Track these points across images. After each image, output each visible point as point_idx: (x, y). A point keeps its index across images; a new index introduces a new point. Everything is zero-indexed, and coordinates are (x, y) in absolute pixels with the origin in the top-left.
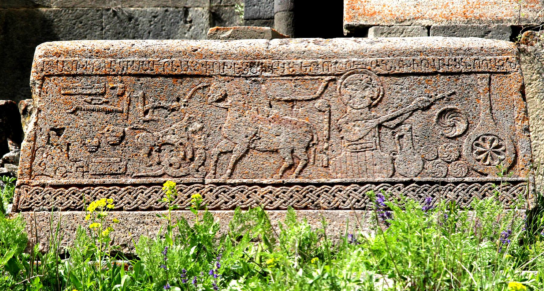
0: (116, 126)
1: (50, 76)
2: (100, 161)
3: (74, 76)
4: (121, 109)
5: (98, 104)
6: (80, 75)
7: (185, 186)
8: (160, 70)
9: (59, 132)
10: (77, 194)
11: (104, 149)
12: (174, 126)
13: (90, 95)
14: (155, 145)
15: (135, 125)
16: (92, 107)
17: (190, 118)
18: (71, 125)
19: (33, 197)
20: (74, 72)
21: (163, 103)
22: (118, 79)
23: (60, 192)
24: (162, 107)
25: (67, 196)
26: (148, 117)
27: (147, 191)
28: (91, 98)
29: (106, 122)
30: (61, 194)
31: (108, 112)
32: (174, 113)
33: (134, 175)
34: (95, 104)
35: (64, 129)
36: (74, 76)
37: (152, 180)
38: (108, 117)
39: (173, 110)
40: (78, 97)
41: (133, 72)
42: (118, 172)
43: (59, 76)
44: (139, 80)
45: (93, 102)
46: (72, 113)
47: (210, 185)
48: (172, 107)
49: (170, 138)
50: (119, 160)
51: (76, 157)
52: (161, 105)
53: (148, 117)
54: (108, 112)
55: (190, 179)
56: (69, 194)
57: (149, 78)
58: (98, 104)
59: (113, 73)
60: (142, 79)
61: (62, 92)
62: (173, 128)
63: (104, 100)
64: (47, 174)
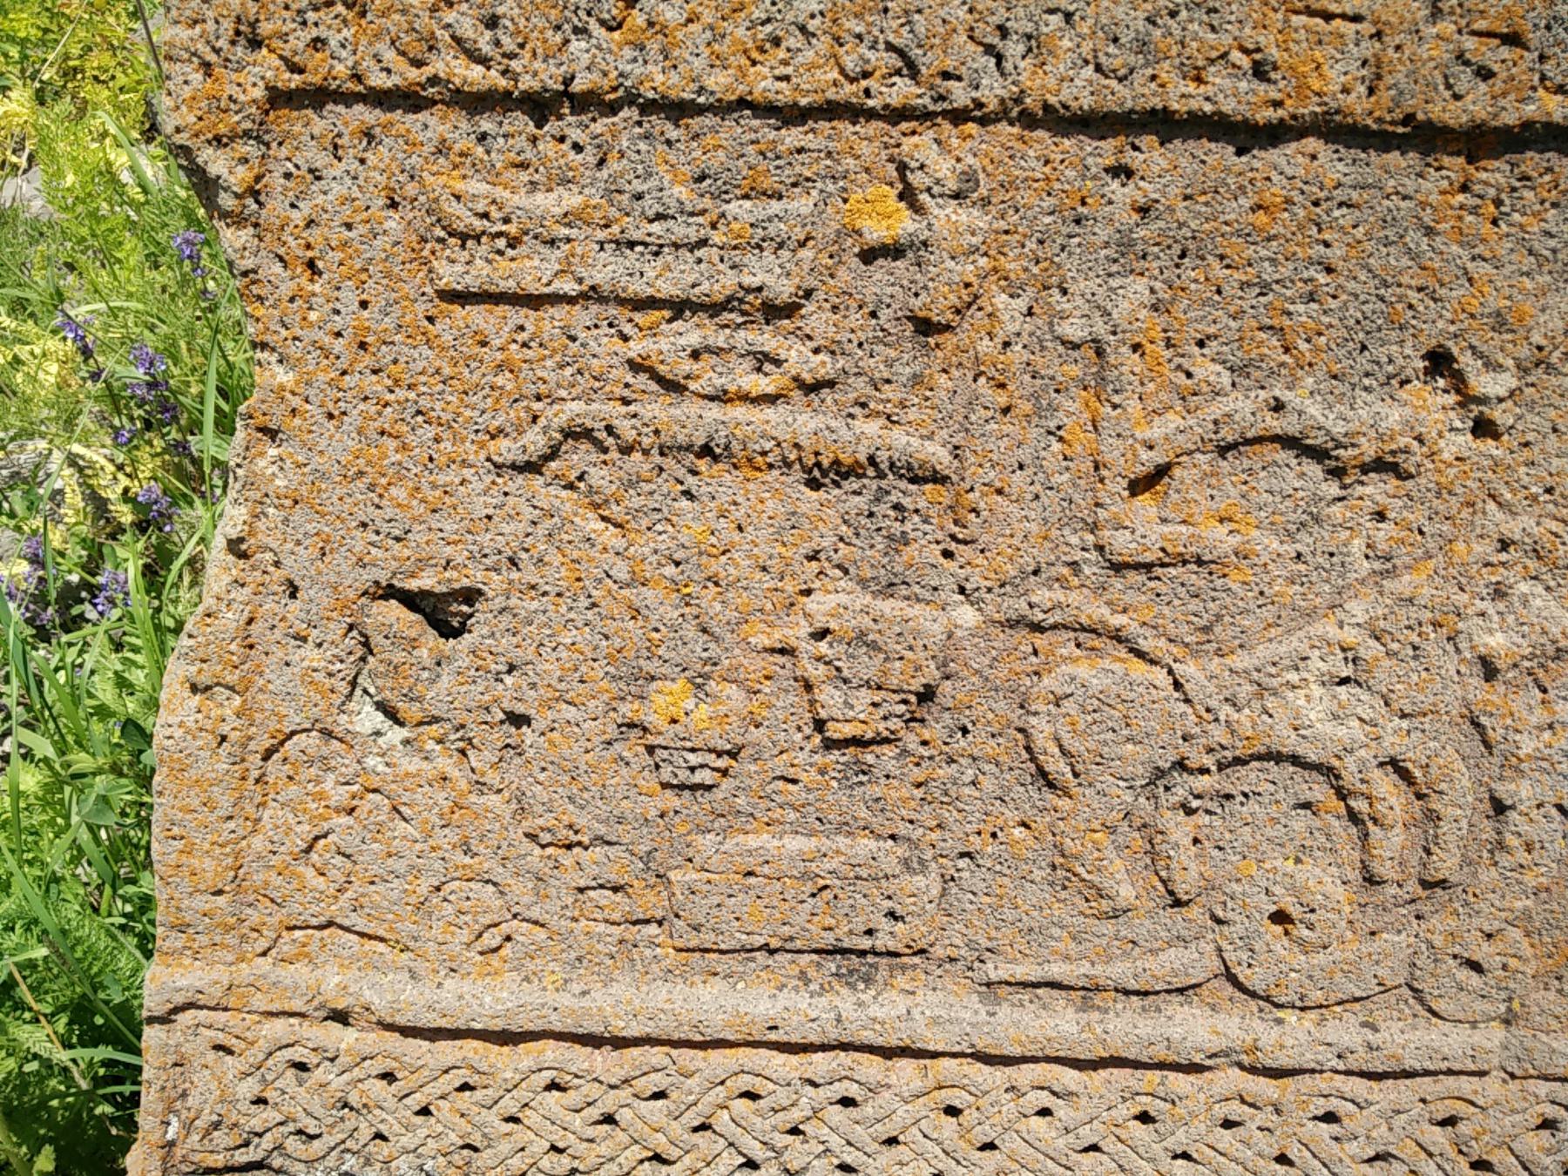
0: (888, 590)
1: (319, 97)
2: (751, 863)
3: (540, 106)
4: (937, 454)
5: (745, 398)
6: (587, 103)
7: (1358, 1086)
8: (1335, 76)
9: (443, 613)
10: (572, 1098)
11: (780, 765)
12: (1358, 610)
13: (679, 308)
14: (1181, 765)
15: (1042, 596)
16: (693, 418)
17: (1504, 545)
18: (530, 575)
19: (270, 1095)
20: (538, 75)
21: (1312, 410)
22: (935, 155)
23: (457, 1077)
24: (1287, 441)
25: (509, 1105)
26: (1144, 526)
27: (1086, 1107)
28: (692, 332)
29: (813, 557)
30: (465, 1087)
31: (824, 473)
32: (1377, 489)
33: (995, 970)
34: (721, 397)
35: (470, 596)
36: (540, 106)
37: (1124, 1028)
38: (824, 512)
39: (1380, 465)
40: (580, 316)
41: (1081, 92)
42: (882, 941)
43: (408, 100)
44: (1122, 172)
45: (709, 377)
46: (531, 467)
47: (1543, 1088)
48: (1369, 450)
49: (1316, 716)
50: (890, 864)
51: (573, 814)
52: (1275, 424)
53: (1144, 526)
54: (824, 473)
55: (1404, 1038)
56: (522, 1094)
57: (1221, 154)
58: (745, 398)
59: (902, 91)
60: (1151, 155)
61: (450, 274)
62: (1350, 636)
63: (800, 359)
64: (360, 923)
